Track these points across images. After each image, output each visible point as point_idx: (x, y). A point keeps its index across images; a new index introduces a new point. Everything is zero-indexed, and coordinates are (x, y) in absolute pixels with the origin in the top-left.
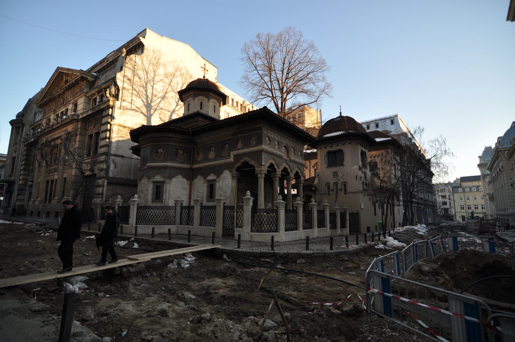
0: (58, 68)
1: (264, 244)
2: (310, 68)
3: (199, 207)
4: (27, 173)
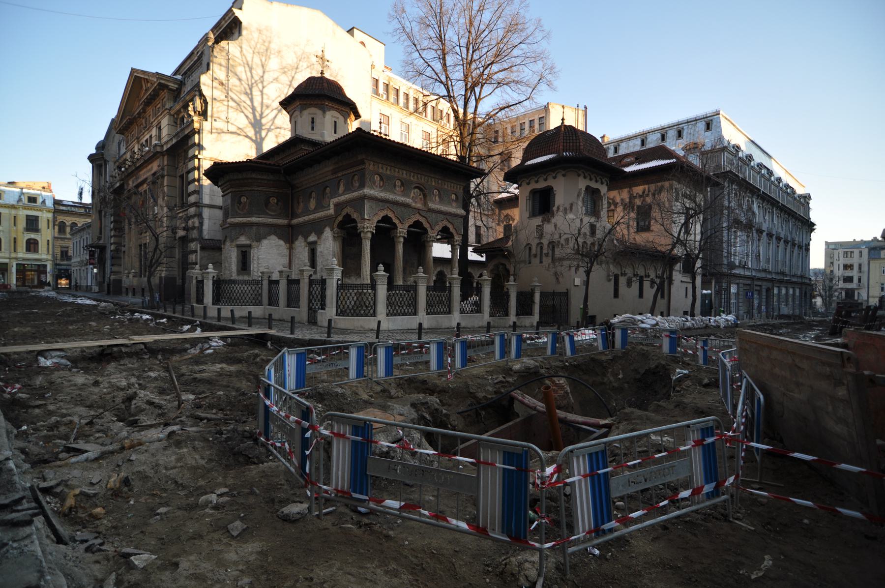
0: (133, 71)
1: (363, 332)
4: (117, 234)
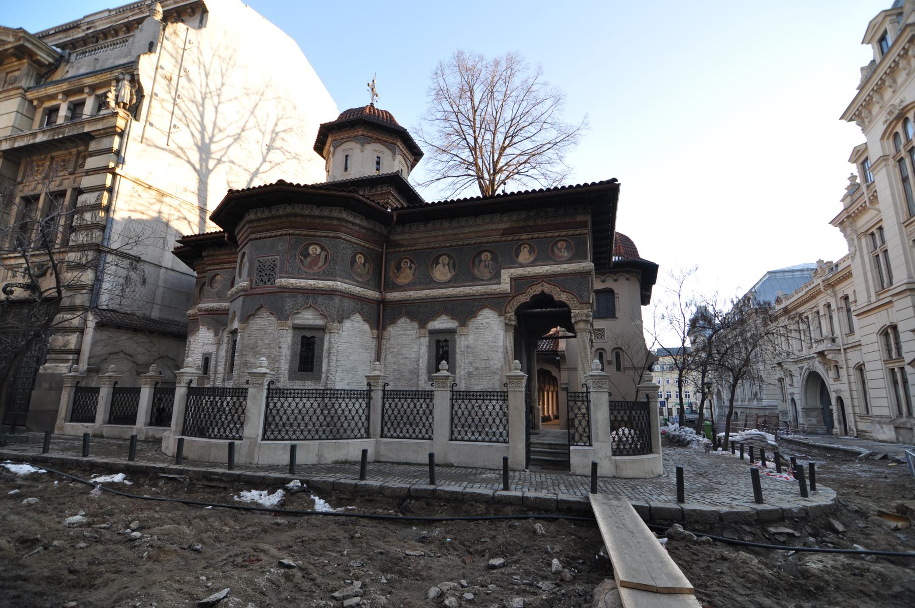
2: (549, 135)
3: (449, 395)
